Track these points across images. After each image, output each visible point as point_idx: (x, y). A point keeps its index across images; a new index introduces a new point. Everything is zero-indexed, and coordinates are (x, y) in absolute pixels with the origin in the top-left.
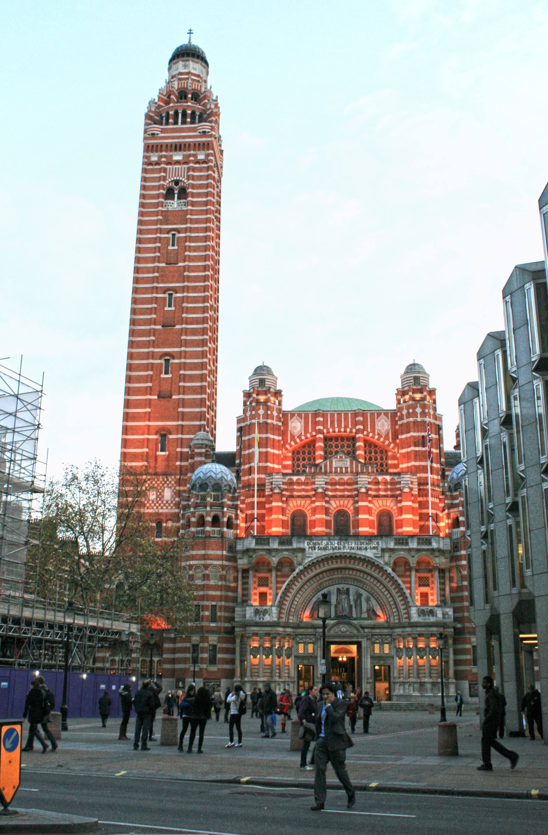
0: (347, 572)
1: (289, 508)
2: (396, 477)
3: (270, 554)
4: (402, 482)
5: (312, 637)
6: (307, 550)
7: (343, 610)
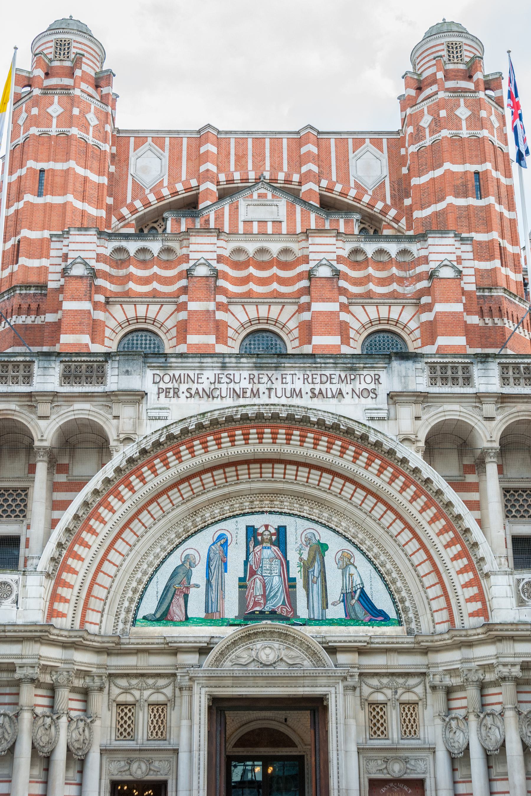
0: (279, 469)
1: (112, 323)
2: (414, 248)
3: (32, 408)
4: (431, 257)
5: (161, 682)
6: (152, 398)
7: (264, 596)
